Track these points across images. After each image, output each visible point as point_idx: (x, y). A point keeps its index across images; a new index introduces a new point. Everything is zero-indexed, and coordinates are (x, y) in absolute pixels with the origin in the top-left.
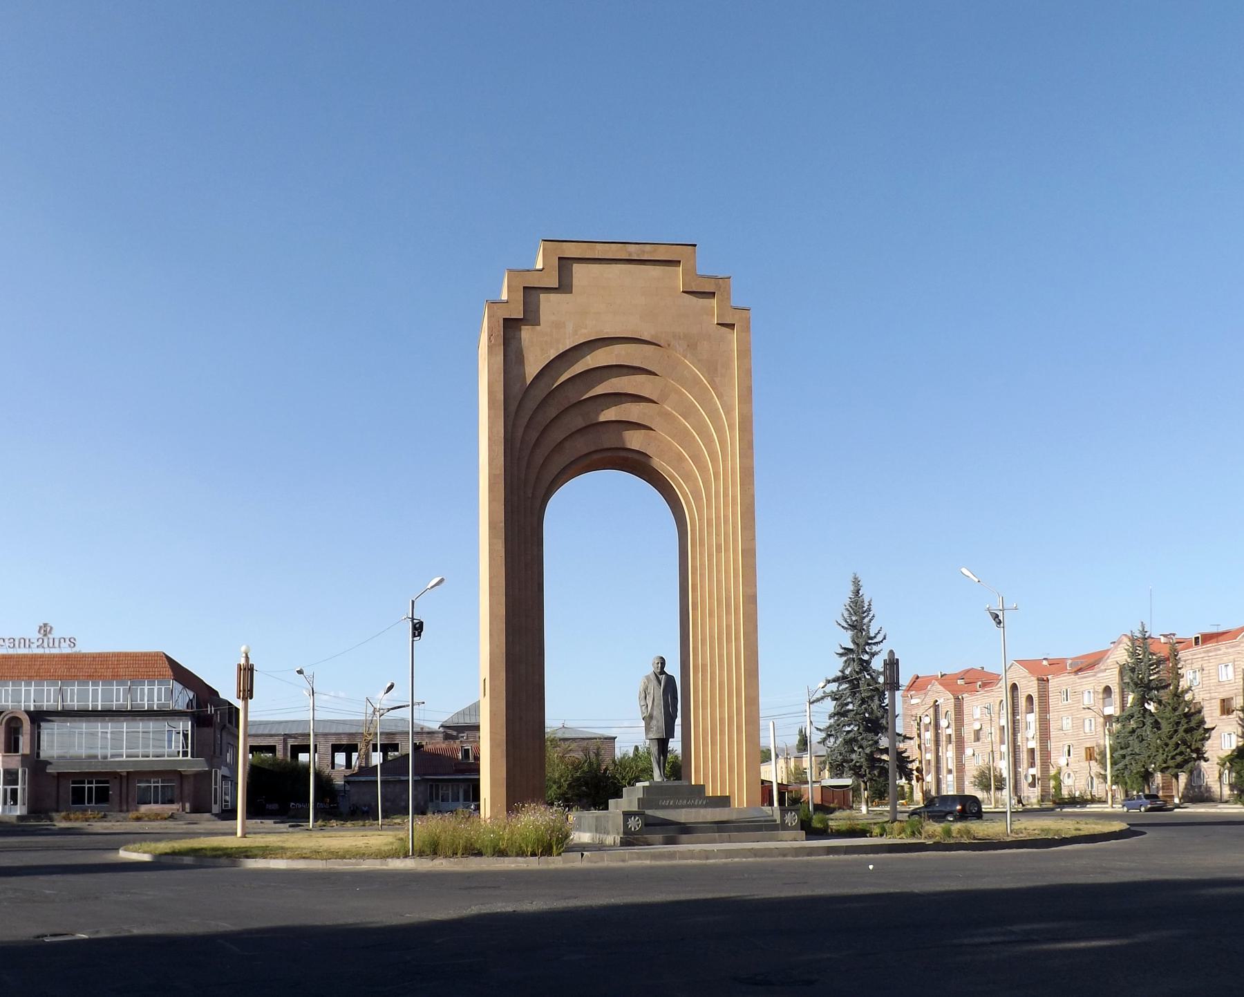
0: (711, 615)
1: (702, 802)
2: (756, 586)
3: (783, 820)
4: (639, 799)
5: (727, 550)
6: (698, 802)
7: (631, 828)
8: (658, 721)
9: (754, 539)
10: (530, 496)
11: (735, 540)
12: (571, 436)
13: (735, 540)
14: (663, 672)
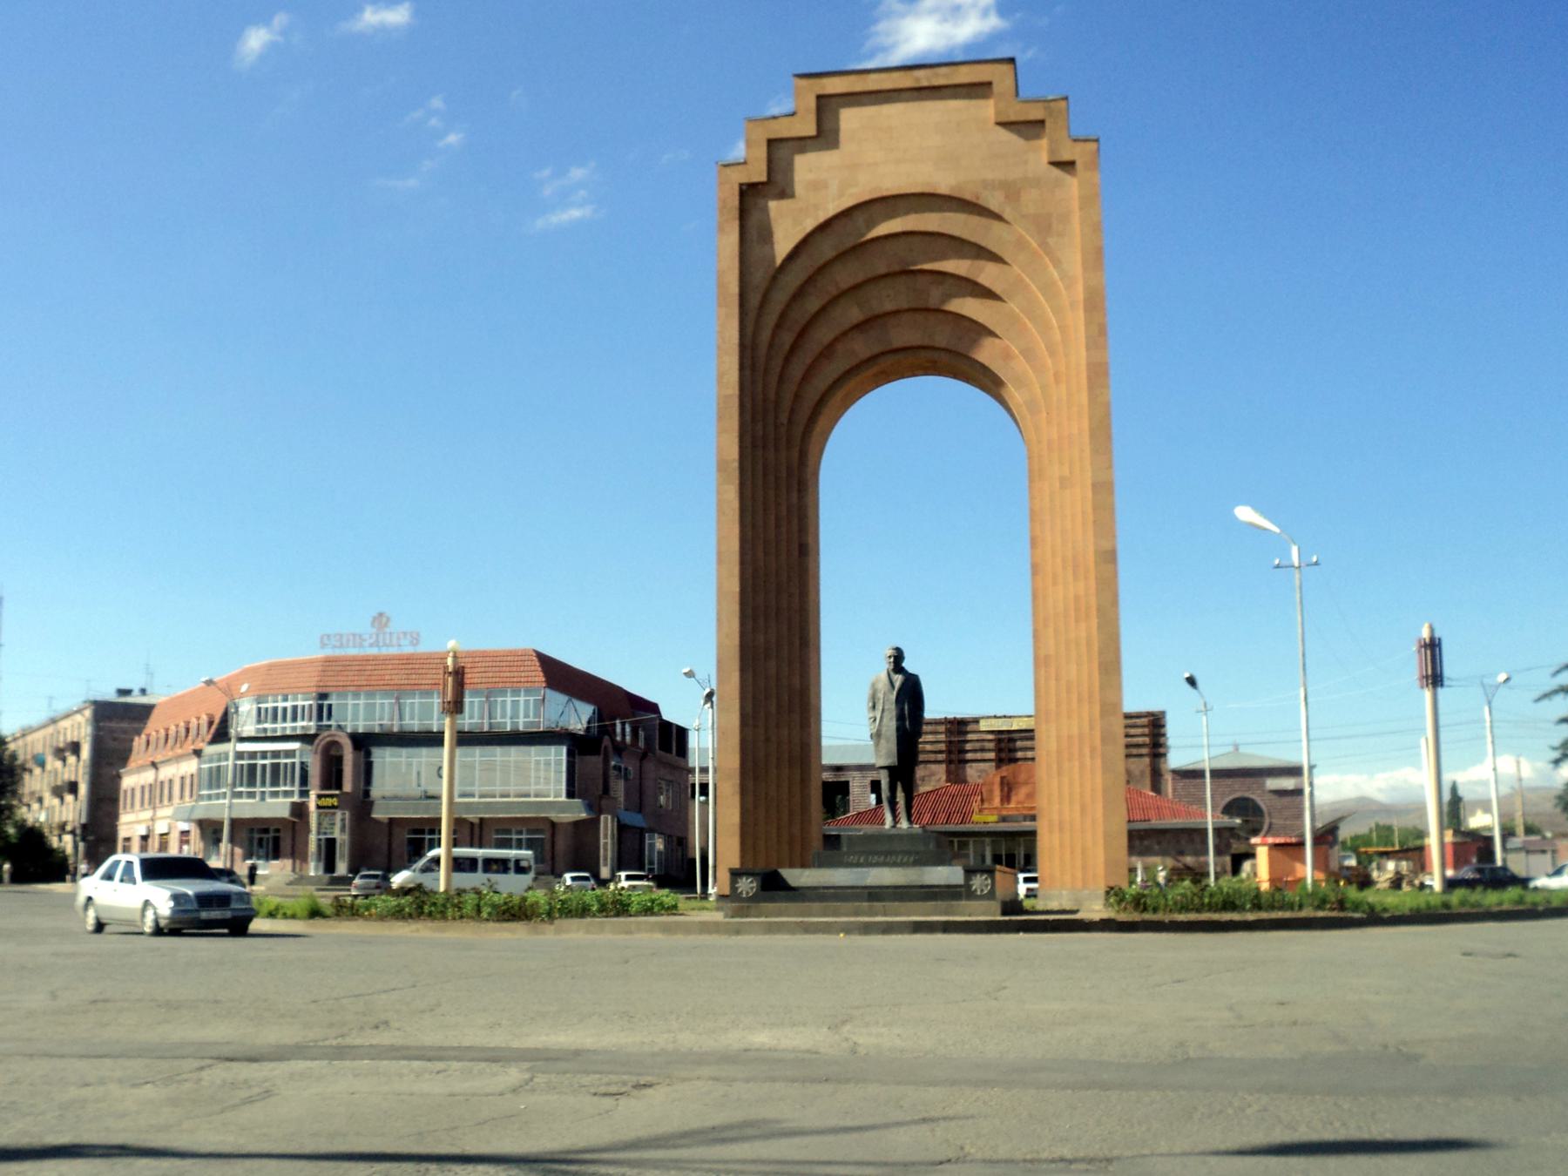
3: (967, 886)
7: (741, 893)
8: (888, 741)
9: (1110, 467)
10: (785, 422)
12: (845, 334)
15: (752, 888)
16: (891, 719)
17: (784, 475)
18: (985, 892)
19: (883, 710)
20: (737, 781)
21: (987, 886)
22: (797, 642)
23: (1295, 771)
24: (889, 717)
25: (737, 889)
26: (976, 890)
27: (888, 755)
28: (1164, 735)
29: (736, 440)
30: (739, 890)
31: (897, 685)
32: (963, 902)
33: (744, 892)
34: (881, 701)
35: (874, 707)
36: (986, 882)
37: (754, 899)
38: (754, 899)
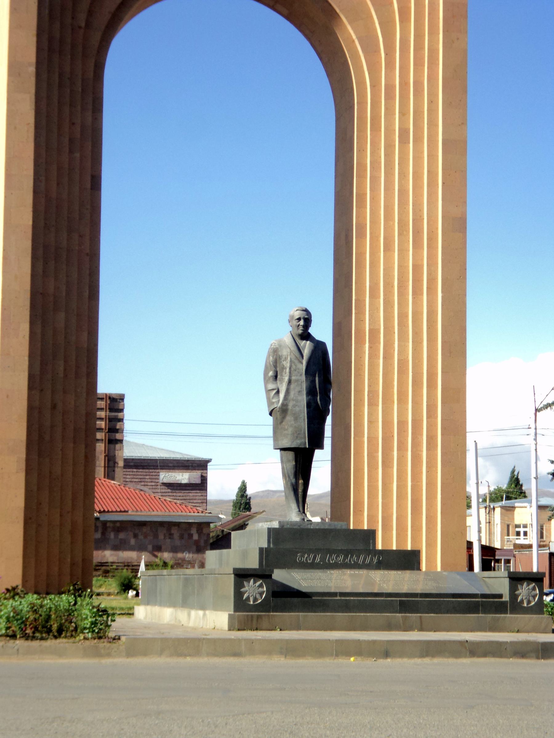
0: (388, 248)
1: (372, 559)
2: (465, 202)
4: (261, 550)
5: (418, 139)
6: (365, 559)
7: (248, 598)
8: (296, 419)
9: (464, 123)
10: (83, 24)
11: (432, 124)
13: (432, 124)
14: (306, 336)
15: (261, 594)
17: (80, 90)
18: (533, 603)
19: (290, 382)
20: (24, 456)
21: (534, 597)
22: (86, 294)
24: (298, 389)
25: (242, 594)
27: (296, 434)
28: (121, 420)
29: (34, 40)
30: (245, 596)
32: (508, 615)
33: (251, 599)
34: (288, 370)
35: (276, 377)
36: (533, 593)
37: (264, 607)
38: (264, 607)
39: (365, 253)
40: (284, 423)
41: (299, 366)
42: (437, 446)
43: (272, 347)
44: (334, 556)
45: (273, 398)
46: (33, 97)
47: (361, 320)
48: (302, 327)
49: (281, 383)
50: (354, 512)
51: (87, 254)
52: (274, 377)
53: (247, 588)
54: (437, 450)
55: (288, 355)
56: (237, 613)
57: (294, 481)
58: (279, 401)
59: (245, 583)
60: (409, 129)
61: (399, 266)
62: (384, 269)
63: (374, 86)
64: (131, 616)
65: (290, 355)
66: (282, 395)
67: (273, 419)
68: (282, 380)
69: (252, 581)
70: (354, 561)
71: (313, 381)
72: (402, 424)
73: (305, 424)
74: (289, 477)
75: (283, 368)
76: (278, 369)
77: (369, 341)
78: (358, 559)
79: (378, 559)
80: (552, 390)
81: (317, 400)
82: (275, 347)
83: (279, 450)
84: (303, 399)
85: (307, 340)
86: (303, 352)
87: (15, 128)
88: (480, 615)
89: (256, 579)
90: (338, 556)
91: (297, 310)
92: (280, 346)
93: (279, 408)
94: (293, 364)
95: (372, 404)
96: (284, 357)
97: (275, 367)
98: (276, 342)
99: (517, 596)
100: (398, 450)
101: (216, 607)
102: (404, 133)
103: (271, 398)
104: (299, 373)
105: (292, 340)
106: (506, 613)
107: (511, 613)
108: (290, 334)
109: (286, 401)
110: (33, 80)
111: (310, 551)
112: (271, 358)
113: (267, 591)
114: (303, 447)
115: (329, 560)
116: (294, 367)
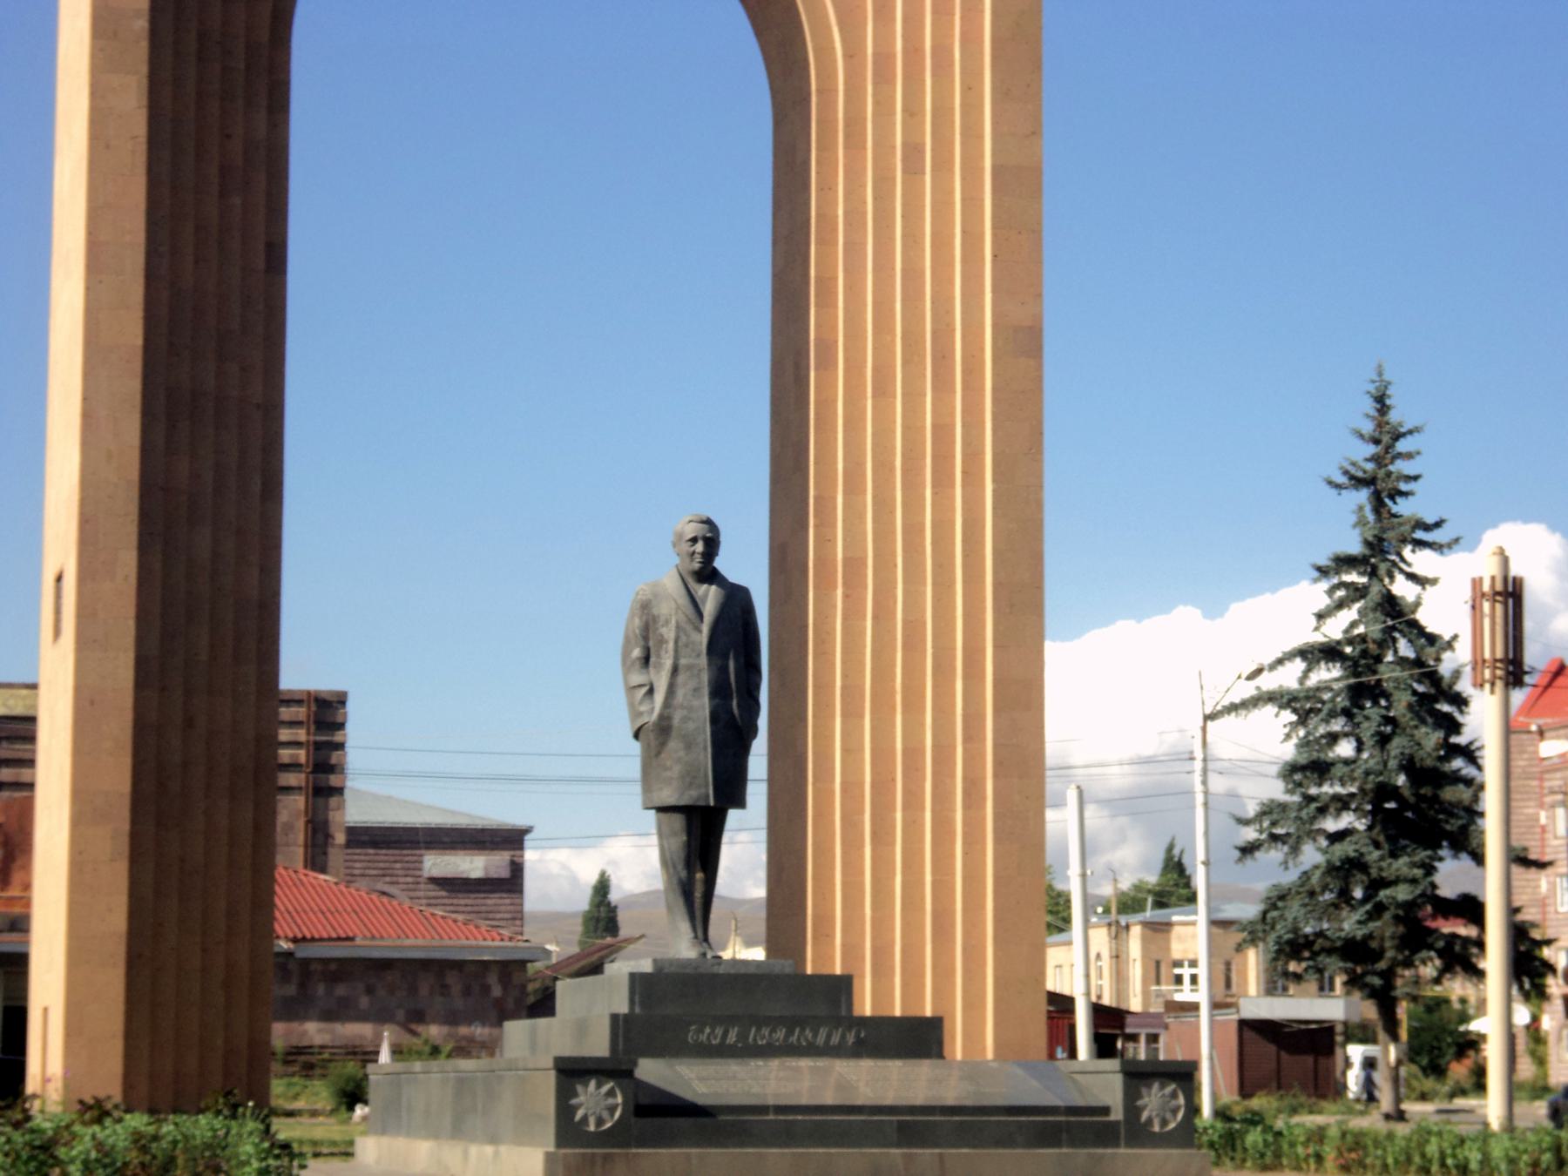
1: (843, 1037)
4: (615, 1018)
6: (829, 1036)
7: (585, 1119)
8: (689, 746)
9: (1036, 133)
14: (708, 574)
16: (696, 690)
17: (242, 66)
18: (1172, 1126)
19: (675, 670)
20: (126, 827)
21: (1175, 1111)
22: (256, 487)
23: (511, 839)
24: (692, 684)
25: (575, 1109)
26: (1150, 1121)
27: (689, 778)
28: (340, 746)
30: (580, 1114)
31: (710, 608)
32: (1122, 1151)
34: (671, 645)
35: (646, 660)
37: (617, 1137)
38: (617, 1137)
39: (835, 401)
40: (663, 755)
41: (695, 636)
42: (984, 799)
43: (639, 597)
44: (766, 1031)
45: (641, 703)
46: (145, 82)
47: (827, 538)
48: (699, 556)
49: (658, 672)
50: (815, 938)
51: (258, 406)
52: (643, 661)
53: (582, 1098)
54: (984, 807)
55: (671, 615)
56: (563, 1151)
57: (684, 874)
58: (653, 709)
59: (579, 1088)
60: (924, 144)
61: (905, 428)
62: (874, 435)
63: (851, 56)
64: (350, 1158)
65: (676, 613)
66: (659, 697)
67: (643, 747)
68: (659, 666)
69: (593, 1084)
70: (806, 1040)
71: (723, 670)
72: (913, 754)
73: (706, 757)
74: (675, 867)
75: (662, 641)
76: (651, 644)
77: (845, 584)
78: (815, 1035)
79: (858, 1034)
80: (1239, 680)
81: (731, 705)
82: (644, 598)
83: (653, 812)
84: (704, 705)
85: (711, 583)
86: (702, 609)
87: (108, 147)
88: (1065, 1150)
89: (603, 1079)
90: (773, 1031)
91: (690, 521)
92: (656, 595)
93: (654, 723)
94: (682, 634)
95: (852, 713)
96: (662, 619)
97: (646, 638)
98: (645, 588)
99: (1139, 1110)
100: (905, 808)
101: (522, 1137)
102: (913, 152)
103: (637, 703)
104: (693, 651)
105: (679, 583)
106: (1117, 1145)
107: (1129, 1145)
108: (675, 570)
109: (668, 711)
110: (143, 47)
111: (716, 1021)
112: (637, 621)
113: (625, 1103)
114: (702, 803)
115: (755, 1040)
116: (683, 639)
